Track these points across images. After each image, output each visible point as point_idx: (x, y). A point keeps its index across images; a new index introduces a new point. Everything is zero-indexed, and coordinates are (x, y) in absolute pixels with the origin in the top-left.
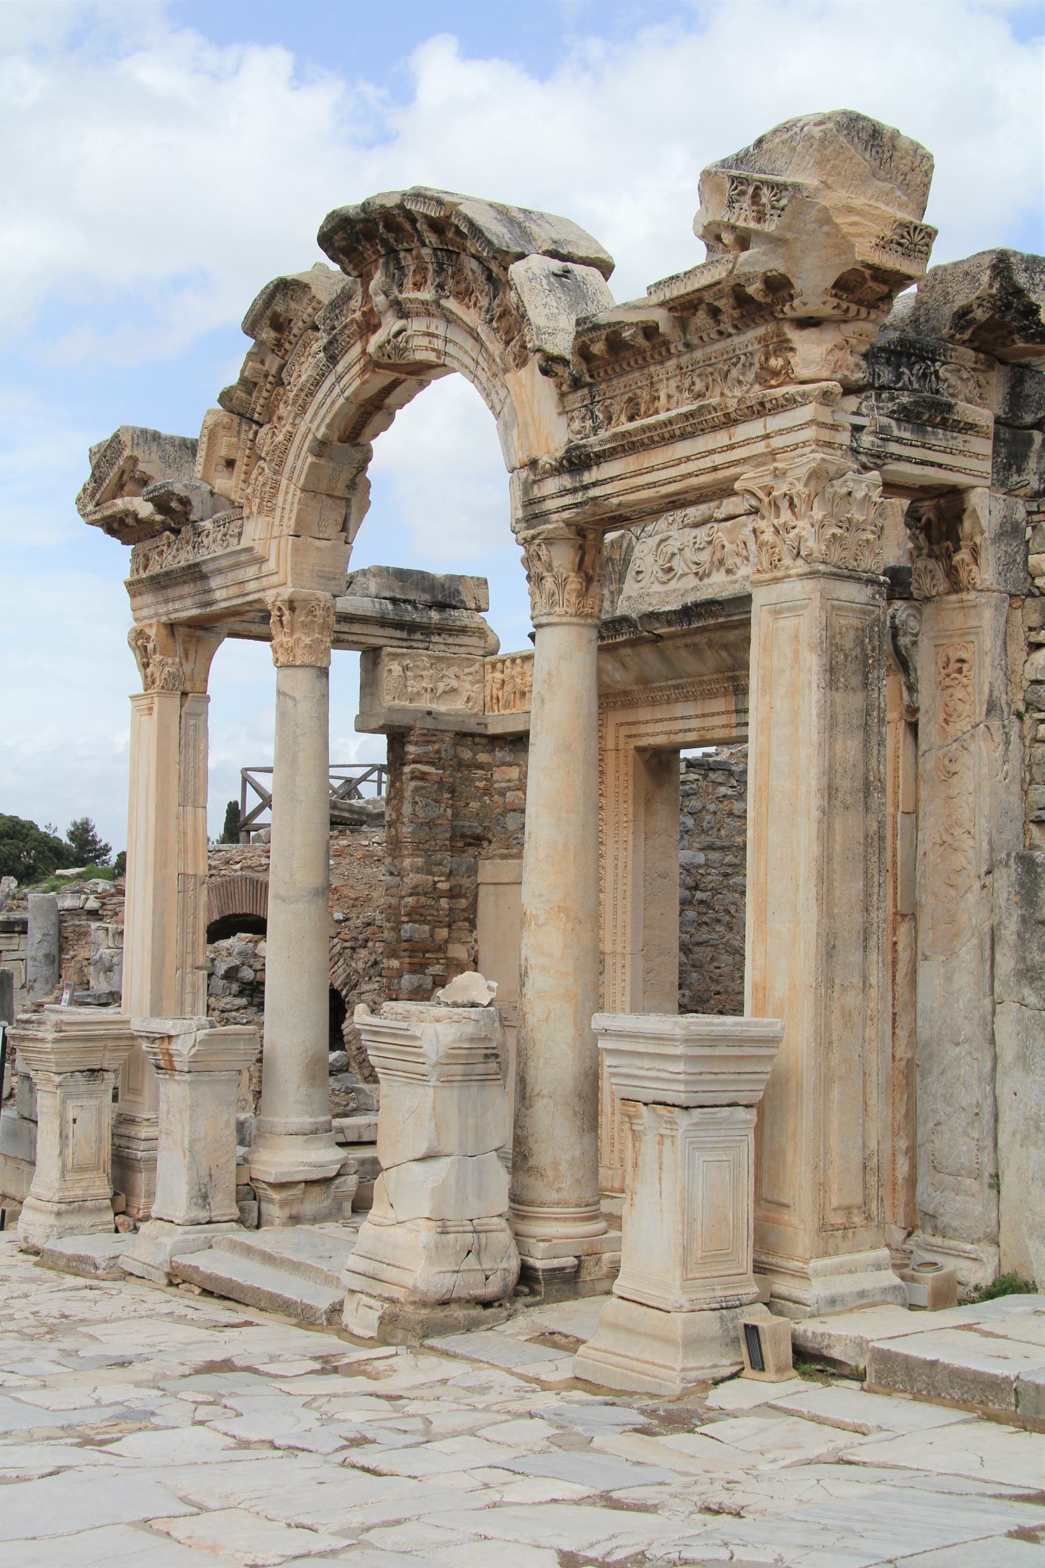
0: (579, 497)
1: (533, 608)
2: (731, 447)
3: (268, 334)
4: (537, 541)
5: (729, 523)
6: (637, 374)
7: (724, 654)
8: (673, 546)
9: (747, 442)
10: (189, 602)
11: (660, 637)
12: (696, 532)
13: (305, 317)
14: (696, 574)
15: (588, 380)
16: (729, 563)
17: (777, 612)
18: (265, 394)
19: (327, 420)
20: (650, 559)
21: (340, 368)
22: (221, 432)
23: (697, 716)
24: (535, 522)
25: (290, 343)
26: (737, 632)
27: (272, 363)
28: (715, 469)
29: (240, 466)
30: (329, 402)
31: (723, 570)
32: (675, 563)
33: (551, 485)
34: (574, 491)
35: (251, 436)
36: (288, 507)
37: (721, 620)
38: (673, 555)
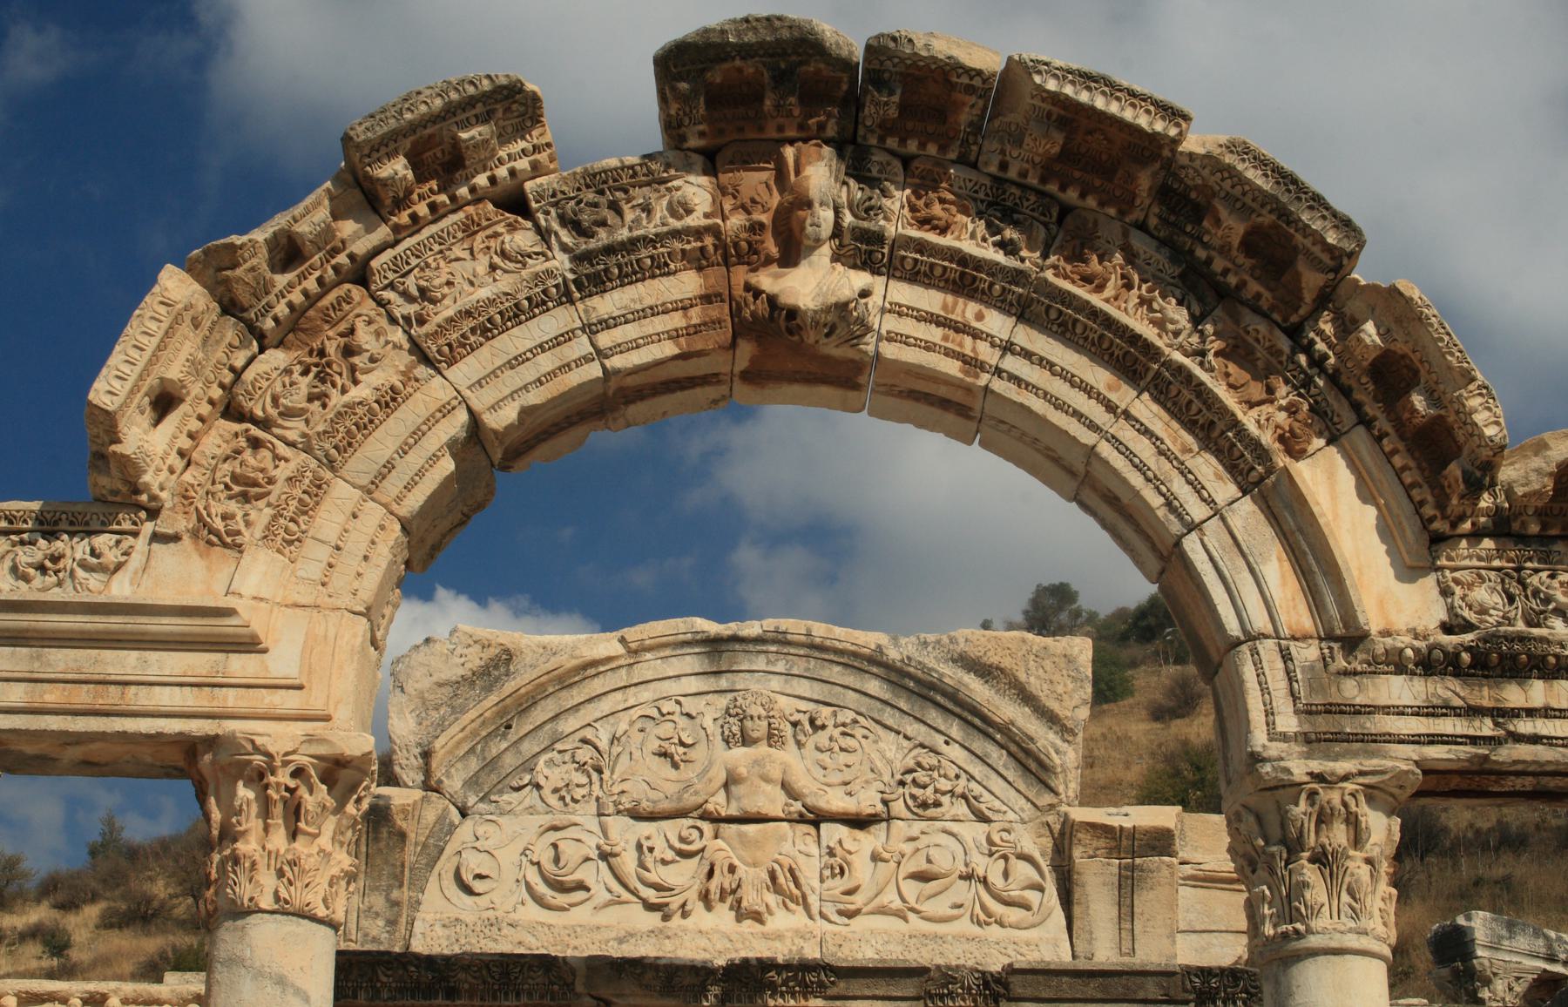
0: (1486, 728)
4: (1349, 786)
15: (1534, 528)
18: (311, 284)
19: (535, 397)
20: (509, 856)
21: (607, 304)
22: (185, 328)
24: (1337, 748)
25: (433, 207)
30: (546, 362)
32: (586, 874)
34: (1473, 712)
35: (239, 363)
36: (356, 543)
38: (588, 859)
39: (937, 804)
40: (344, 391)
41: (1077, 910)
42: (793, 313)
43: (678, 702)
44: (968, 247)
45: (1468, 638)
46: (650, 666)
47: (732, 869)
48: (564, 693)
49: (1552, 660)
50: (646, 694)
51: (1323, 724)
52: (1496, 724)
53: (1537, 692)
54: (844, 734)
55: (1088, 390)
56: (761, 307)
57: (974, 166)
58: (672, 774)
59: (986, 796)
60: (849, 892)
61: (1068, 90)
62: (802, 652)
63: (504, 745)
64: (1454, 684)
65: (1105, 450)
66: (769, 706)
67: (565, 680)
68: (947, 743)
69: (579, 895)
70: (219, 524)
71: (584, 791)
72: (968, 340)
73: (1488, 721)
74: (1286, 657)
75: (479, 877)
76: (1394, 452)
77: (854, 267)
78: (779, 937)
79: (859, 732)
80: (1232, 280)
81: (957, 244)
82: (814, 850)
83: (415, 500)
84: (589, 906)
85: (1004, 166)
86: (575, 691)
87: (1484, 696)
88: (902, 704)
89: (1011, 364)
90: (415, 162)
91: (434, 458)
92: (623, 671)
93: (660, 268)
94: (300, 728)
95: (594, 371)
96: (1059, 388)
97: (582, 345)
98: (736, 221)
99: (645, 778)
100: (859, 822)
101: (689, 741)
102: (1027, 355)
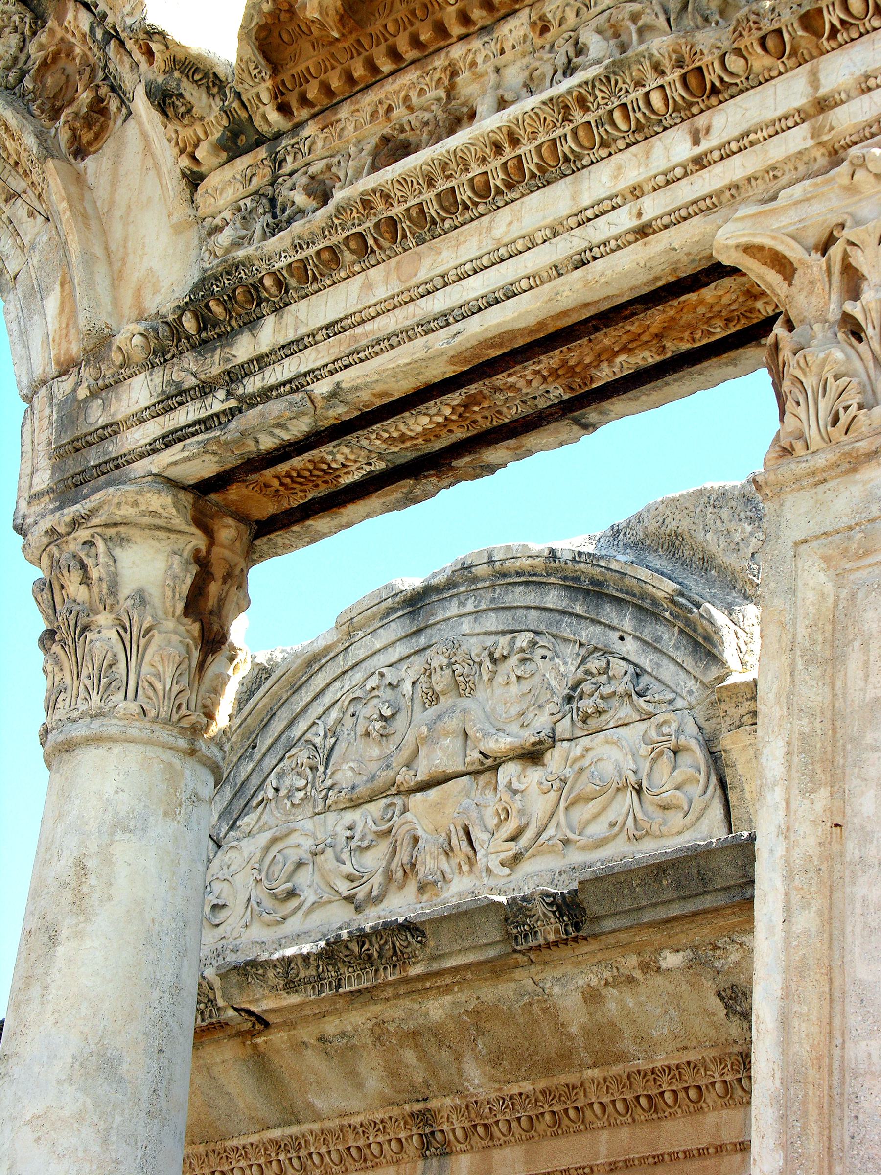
0: (217, 403)
1: (51, 705)
2: (700, 163)
4: (83, 534)
5: (433, 794)
6: (411, 76)
7: (409, 1056)
8: (301, 843)
9: (744, 142)
11: (262, 1022)
12: (349, 817)
14: (349, 899)
20: (244, 881)
26: (449, 998)
31: (412, 887)
34: (205, 389)
41: (732, 796)
43: (382, 675)
47: (416, 840)
48: (296, 696)
49: (268, 282)
50: (358, 676)
52: (229, 394)
53: (270, 333)
54: (524, 660)
58: (376, 752)
59: (655, 686)
60: (513, 838)
62: (487, 584)
63: (251, 766)
64: (189, 361)
68: (622, 638)
69: (294, 903)
71: (302, 794)
73: (221, 394)
86: (303, 691)
87: (214, 366)
88: (579, 609)
92: (341, 657)
100: (533, 756)
101: (387, 713)
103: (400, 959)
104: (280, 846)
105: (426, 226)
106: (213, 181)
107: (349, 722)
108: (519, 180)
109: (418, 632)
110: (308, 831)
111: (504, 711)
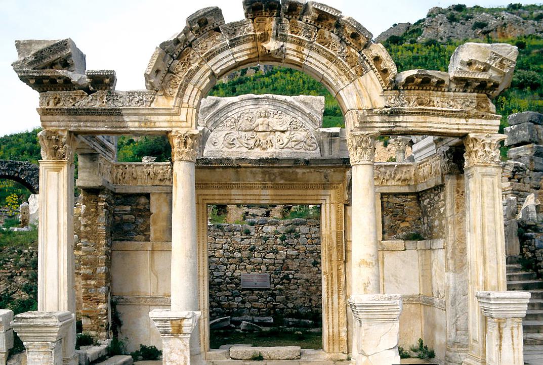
0: (392, 125)
2: (467, 124)
3: (197, 26)
4: (367, 136)
5: (264, 133)
6: (424, 92)
10: (101, 124)
12: (244, 133)
13: (215, 25)
14: (247, 147)
16: (264, 146)
17: (484, 175)
19: (223, 67)
20: (221, 139)
21: (235, 49)
23: (243, 195)
25: (203, 32)
27: (191, 36)
28: (458, 129)
29: (161, 74)
30: (225, 60)
32: (235, 142)
33: (377, 118)
34: (389, 122)
37: (277, 165)
39: (297, 128)
40: (189, 67)
42: (269, 51)
44: (301, 37)
45: (389, 109)
46: (245, 103)
47: (260, 141)
50: (243, 109)
51: (364, 125)
53: (401, 118)
55: (322, 64)
56: (264, 50)
57: (302, 21)
58: (249, 123)
61: (319, 8)
64: (386, 117)
65: (325, 75)
66: (266, 111)
67: (228, 106)
70: (168, 93)
72: (301, 54)
73: (392, 124)
74: (357, 113)
75: (215, 143)
76: (378, 75)
77: (280, 41)
78: (268, 153)
79: (282, 115)
80: (349, 42)
81: (299, 37)
82: (274, 137)
83: (203, 87)
84: (235, 148)
85: (307, 21)
89: (309, 59)
90: (199, 23)
91: (206, 80)
93: (244, 42)
94: (186, 129)
95: (233, 62)
96: (317, 63)
97: (231, 57)
98: (258, 33)
99: (244, 124)
100: (283, 132)
102: (311, 57)
103: (274, 163)
104: (228, 135)
105: (428, 114)
106: (389, 91)
107: (242, 117)
108: (443, 116)
109: (256, 105)
110: (235, 134)
111: (275, 123)
